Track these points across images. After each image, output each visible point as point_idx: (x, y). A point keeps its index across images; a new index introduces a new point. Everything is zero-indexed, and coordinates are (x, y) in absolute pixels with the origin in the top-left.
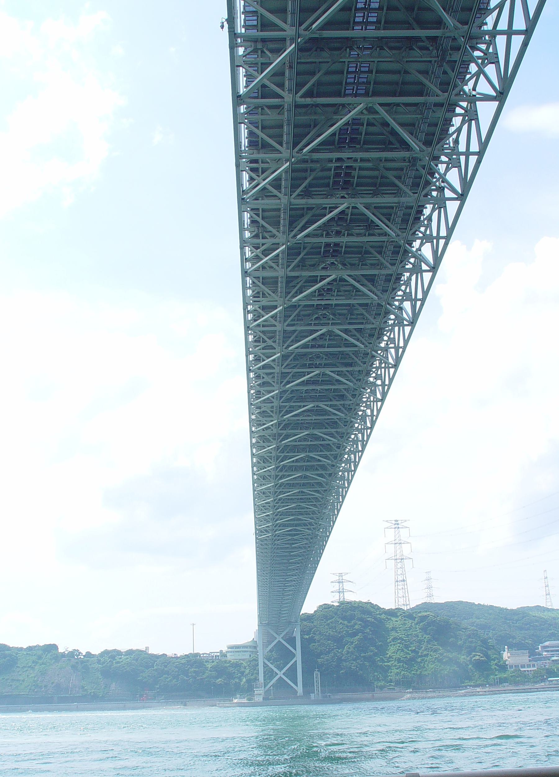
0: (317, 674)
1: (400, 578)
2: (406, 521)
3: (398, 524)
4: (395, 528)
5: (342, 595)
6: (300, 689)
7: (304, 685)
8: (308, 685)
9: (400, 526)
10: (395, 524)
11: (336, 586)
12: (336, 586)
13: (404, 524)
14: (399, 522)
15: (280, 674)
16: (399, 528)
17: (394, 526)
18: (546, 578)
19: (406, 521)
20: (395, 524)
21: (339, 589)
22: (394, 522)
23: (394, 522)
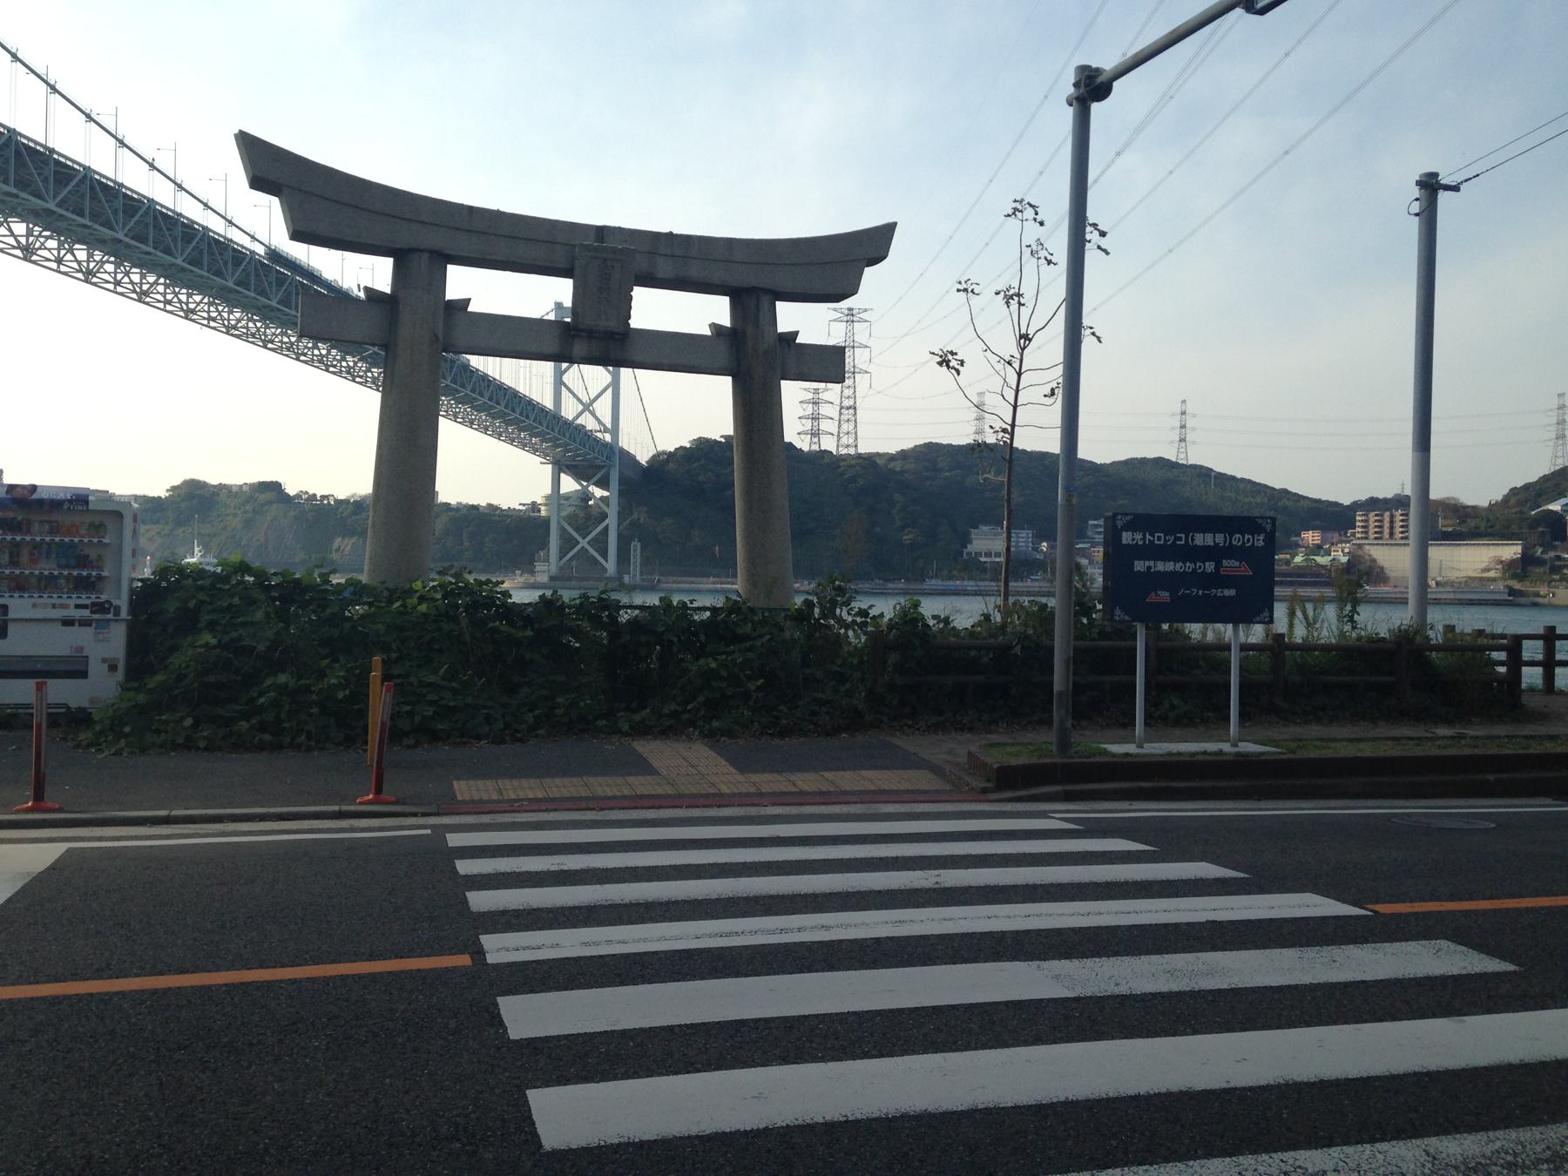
0: (636, 547)
1: (846, 403)
2: (866, 310)
3: (853, 315)
4: (847, 322)
5: (816, 424)
6: (611, 566)
7: (618, 563)
8: (623, 558)
9: (855, 319)
10: (848, 315)
11: (809, 409)
12: (809, 409)
13: (863, 316)
14: (854, 312)
15: (583, 543)
16: (853, 321)
17: (845, 319)
18: (1183, 413)
19: (866, 310)
20: (848, 315)
21: (813, 414)
22: (846, 312)
23: (846, 312)
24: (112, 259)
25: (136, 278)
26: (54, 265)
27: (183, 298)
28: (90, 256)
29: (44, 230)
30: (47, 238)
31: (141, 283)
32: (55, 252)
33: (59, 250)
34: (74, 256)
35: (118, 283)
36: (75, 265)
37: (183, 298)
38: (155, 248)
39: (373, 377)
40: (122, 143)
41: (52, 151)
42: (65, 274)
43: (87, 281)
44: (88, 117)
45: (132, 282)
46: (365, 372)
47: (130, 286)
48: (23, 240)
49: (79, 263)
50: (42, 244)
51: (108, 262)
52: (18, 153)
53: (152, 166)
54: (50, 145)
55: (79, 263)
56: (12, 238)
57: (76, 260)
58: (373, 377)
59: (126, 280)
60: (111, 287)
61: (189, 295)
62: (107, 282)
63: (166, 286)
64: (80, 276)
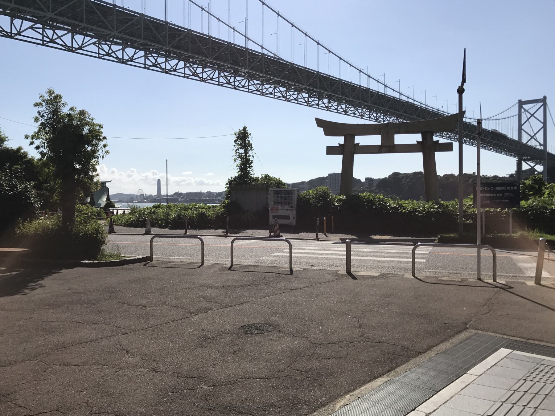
24: (368, 111)
25: (375, 115)
26: (353, 115)
27: (389, 119)
28: (362, 110)
29: (350, 105)
30: (351, 107)
31: (377, 116)
32: (353, 111)
33: (354, 110)
34: (358, 111)
35: (370, 117)
36: (358, 114)
37: (389, 119)
38: (379, 106)
39: (449, 136)
40: (369, 76)
41: (351, 83)
42: (356, 117)
43: (362, 118)
44: (360, 71)
45: (374, 117)
46: (455, 137)
47: (373, 118)
48: (345, 109)
49: (359, 113)
50: (350, 109)
51: (367, 112)
52: (342, 85)
53: (378, 81)
54: (350, 81)
55: (359, 113)
56: (323, 104)
57: (359, 113)
58: (449, 136)
59: (372, 116)
60: (368, 119)
61: (390, 118)
62: (367, 117)
63: (383, 116)
64: (360, 117)
